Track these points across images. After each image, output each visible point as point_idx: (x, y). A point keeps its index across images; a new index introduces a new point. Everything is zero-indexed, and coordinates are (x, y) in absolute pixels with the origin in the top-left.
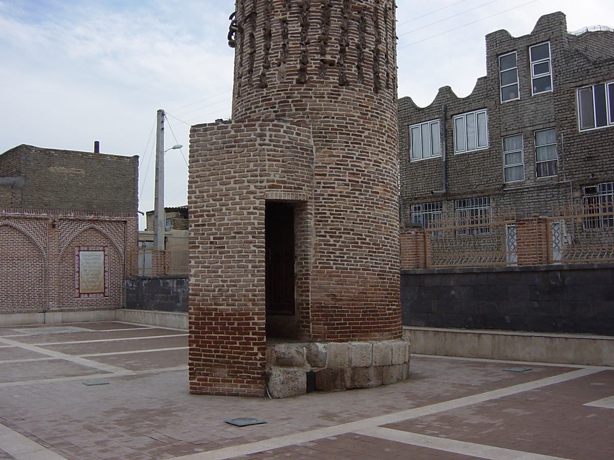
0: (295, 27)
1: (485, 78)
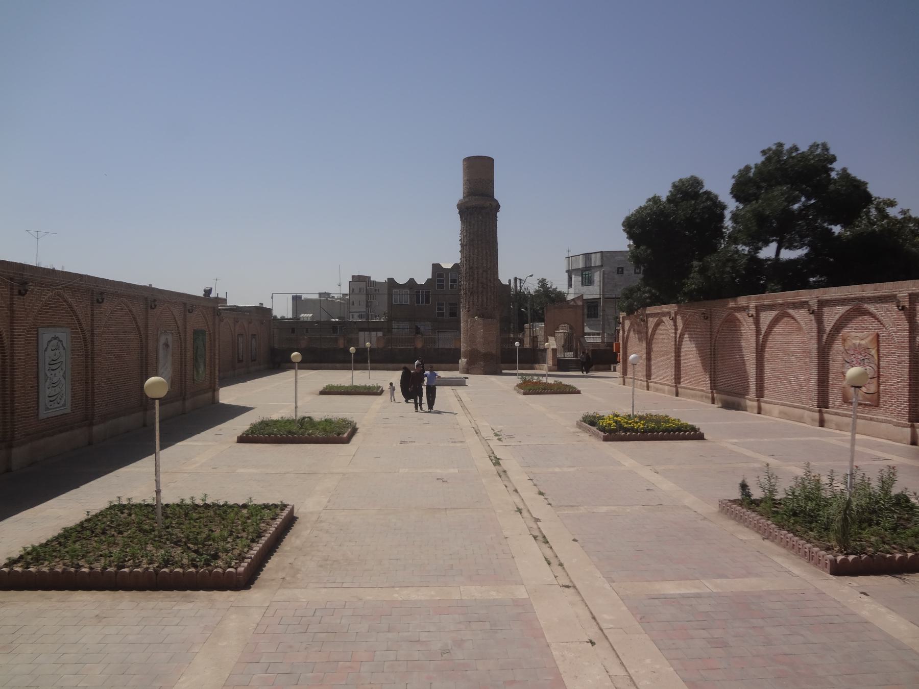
0: (492, 298)
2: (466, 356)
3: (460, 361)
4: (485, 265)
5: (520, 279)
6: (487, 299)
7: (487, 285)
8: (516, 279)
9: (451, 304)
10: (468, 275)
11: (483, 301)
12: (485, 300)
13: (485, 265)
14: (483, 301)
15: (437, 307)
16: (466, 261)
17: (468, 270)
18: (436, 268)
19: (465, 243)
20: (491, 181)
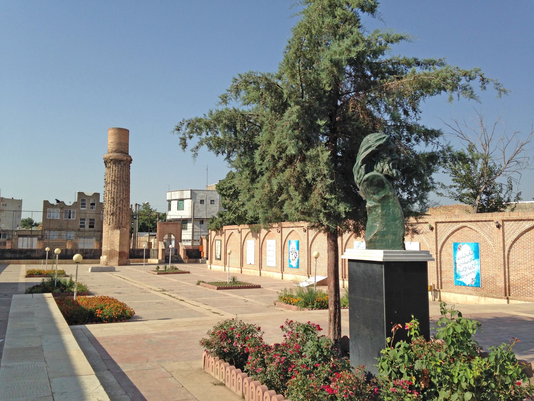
0: (126, 217)
1: (76, 202)
2: (106, 254)
3: (101, 257)
4: (122, 196)
5: (139, 205)
6: (122, 217)
7: (123, 209)
8: (136, 204)
9: (90, 220)
10: (110, 202)
11: (119, 219)
12: (121, 218)
13: (122, 196)
14: (119, 219)
15: (80, 221)
16: (109, 193)
17: (110, 199)
18: (81, 195)
19: (108, 182)
20: (127, 144)
